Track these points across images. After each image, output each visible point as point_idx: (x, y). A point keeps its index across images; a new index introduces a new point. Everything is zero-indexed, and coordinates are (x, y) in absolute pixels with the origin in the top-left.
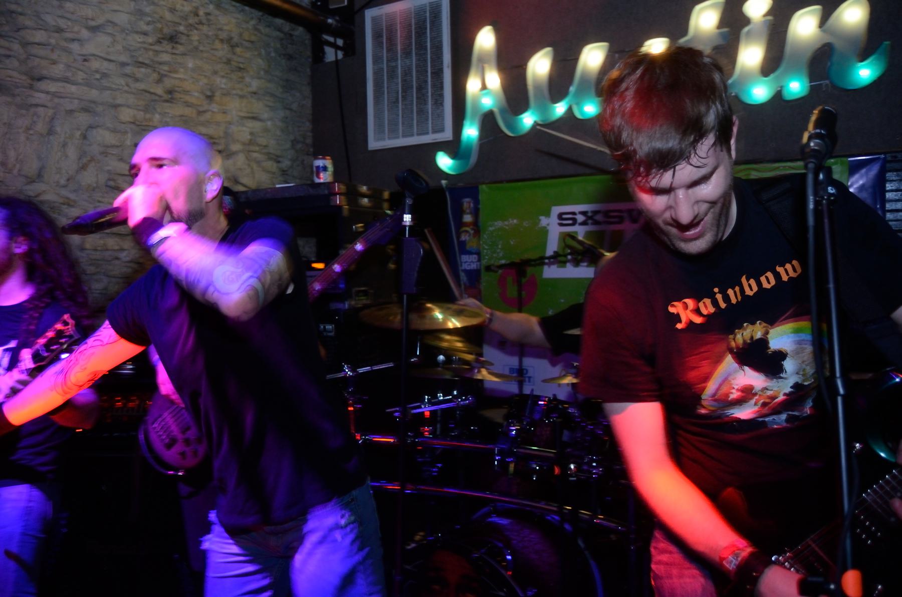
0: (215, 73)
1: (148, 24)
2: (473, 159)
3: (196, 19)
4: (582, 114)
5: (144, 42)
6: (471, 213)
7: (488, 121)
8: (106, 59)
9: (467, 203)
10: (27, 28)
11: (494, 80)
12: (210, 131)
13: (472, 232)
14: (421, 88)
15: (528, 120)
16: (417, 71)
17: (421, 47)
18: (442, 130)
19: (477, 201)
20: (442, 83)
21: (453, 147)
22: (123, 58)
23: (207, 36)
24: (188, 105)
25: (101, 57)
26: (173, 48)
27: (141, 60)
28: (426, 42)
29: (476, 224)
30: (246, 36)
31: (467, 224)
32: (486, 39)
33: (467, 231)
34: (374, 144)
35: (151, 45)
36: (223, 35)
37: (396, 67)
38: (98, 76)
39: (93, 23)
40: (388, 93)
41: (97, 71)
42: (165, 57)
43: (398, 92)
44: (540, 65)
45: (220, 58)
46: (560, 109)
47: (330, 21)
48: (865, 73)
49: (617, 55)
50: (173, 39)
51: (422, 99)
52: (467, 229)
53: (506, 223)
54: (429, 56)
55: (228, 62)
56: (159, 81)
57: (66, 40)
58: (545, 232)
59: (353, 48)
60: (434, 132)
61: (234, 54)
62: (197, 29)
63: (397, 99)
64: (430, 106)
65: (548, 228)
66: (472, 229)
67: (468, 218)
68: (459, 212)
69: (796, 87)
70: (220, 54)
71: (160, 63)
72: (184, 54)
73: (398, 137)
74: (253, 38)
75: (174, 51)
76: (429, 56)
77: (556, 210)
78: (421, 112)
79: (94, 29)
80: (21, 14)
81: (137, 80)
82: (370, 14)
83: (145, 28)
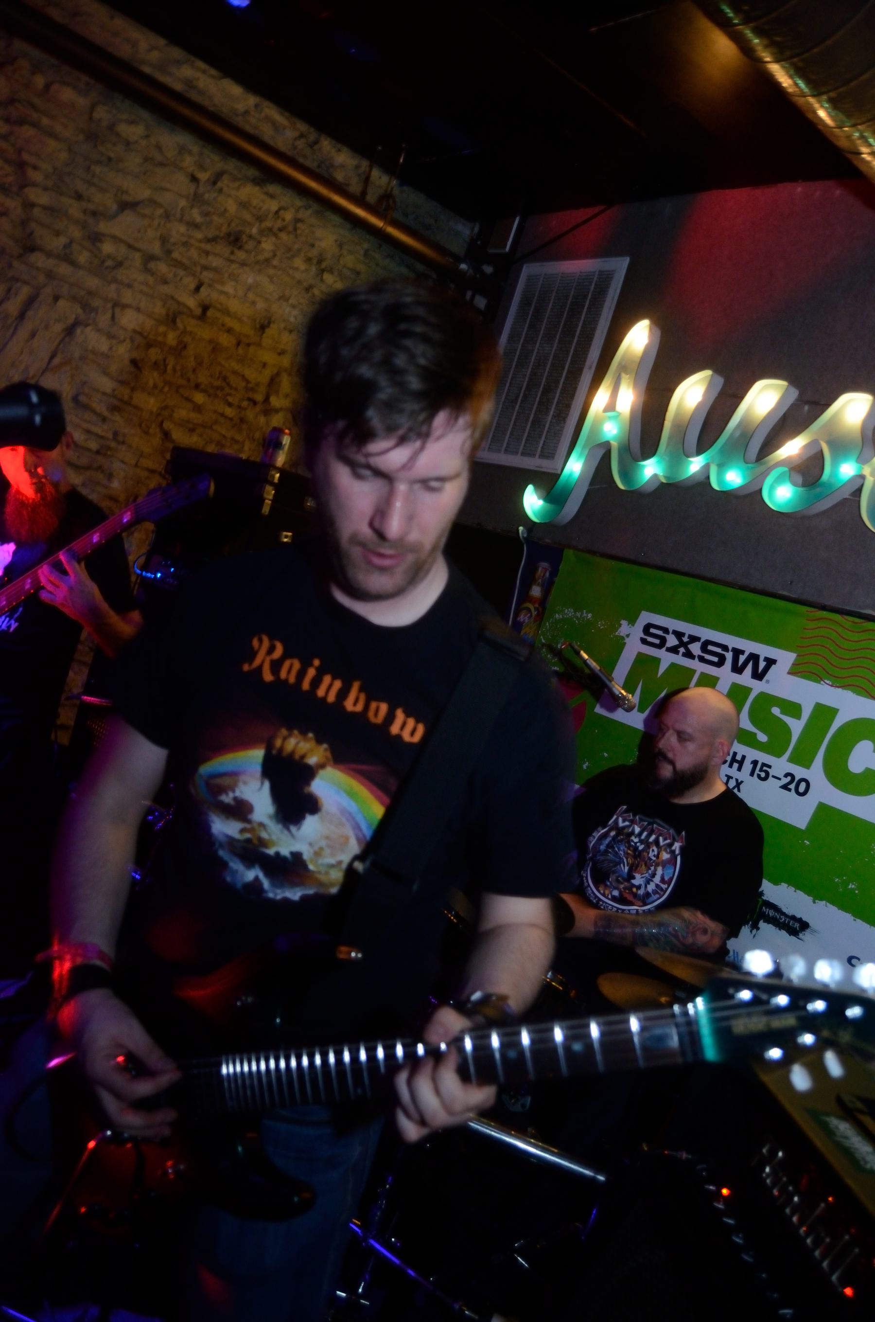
0: (283, 298)
1: (206, 214)
2: (572, 508)
3: (279, 224)
4: (720, 480)
5: (190, 237)
6: (542, 586)
7: (602, 458)
8: (130, 246)
9: (543, 569)
10: (34, 185)
12: (251, 374)
13: (534, 613)
14: (548, 390)
15: (651, 469)
16: (553, 365)
17: (569, 331)
19: (554, 572)
20: (575, 389)
22: (156, 248)
23: (289, 250)
24: (229, 331)
25: (124, 242)
26: (232, 253)
27: (175, 255)
28: (577, 325)
29: (543, 602)
30: (349, 260)
31: (531, 600)
32: (639, 337)
33: (529, 610)
35: (200, 241)
36: (314, 253)
37: (532, 351)
38: (109, 263)
39: (125, 198)
40: (510, 386)
41: (109, 256)
42: (215, 262)
43: (521, 388)
44: (692, 393)
45: (299, 282)
46: (695, 465)
47: (463, 266)
49: (806, 408)
50: (235, 240)
51: (544, 406)
52: (532, 609)
53: (578, 614)
54: (573, 347)
55: (308, 289)
56: (197, 289)
57: (85, 212)
58: (620, 645)
59: (494, 314)
60: (542, 456)
61: (322, 280)
62: (275, 235)
64: (549, 418)
65: (627, 640)
66: (536, 609)
67: (536, 591)
68: (529, 580)
70: (298, 276)
71: (205, 268)
72: (243, 264)
73: (499, 451)
74: (361, 267)
75: (232, 257)
76: (573, 347)
77: (646, 617)
78: (537, 423)
79: (125, 206)
80: (35, 168)
81: (165, 282)
82: (528, 270)
83: (198, 219)
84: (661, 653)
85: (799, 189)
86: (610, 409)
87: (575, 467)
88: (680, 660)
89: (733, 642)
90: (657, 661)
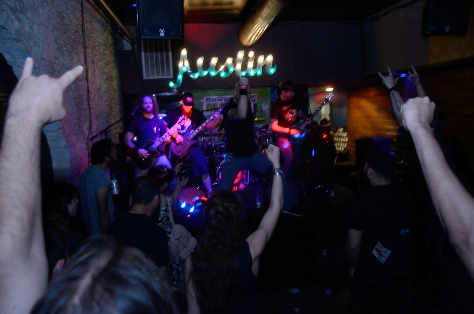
7: (186, 75)
11: (187, 63)
14: (162, 62)
15: (197, 75)
18: (170, 75)
21: (175, 80)
32: (184, 52)
34: (145, 77)
44: (200, 61)
46: (205, 73)
48: (272, 71)
58: (202, 103)
60: (167, 75)
63: (153, 65)
69: (259, 72)
77: (205, 98)
84: (211, 102)
85: (203, 24)
86: (184, 66)
87: (180, 77)
88: (214, 102)
89: (223, 97)
90: (211, 104)
